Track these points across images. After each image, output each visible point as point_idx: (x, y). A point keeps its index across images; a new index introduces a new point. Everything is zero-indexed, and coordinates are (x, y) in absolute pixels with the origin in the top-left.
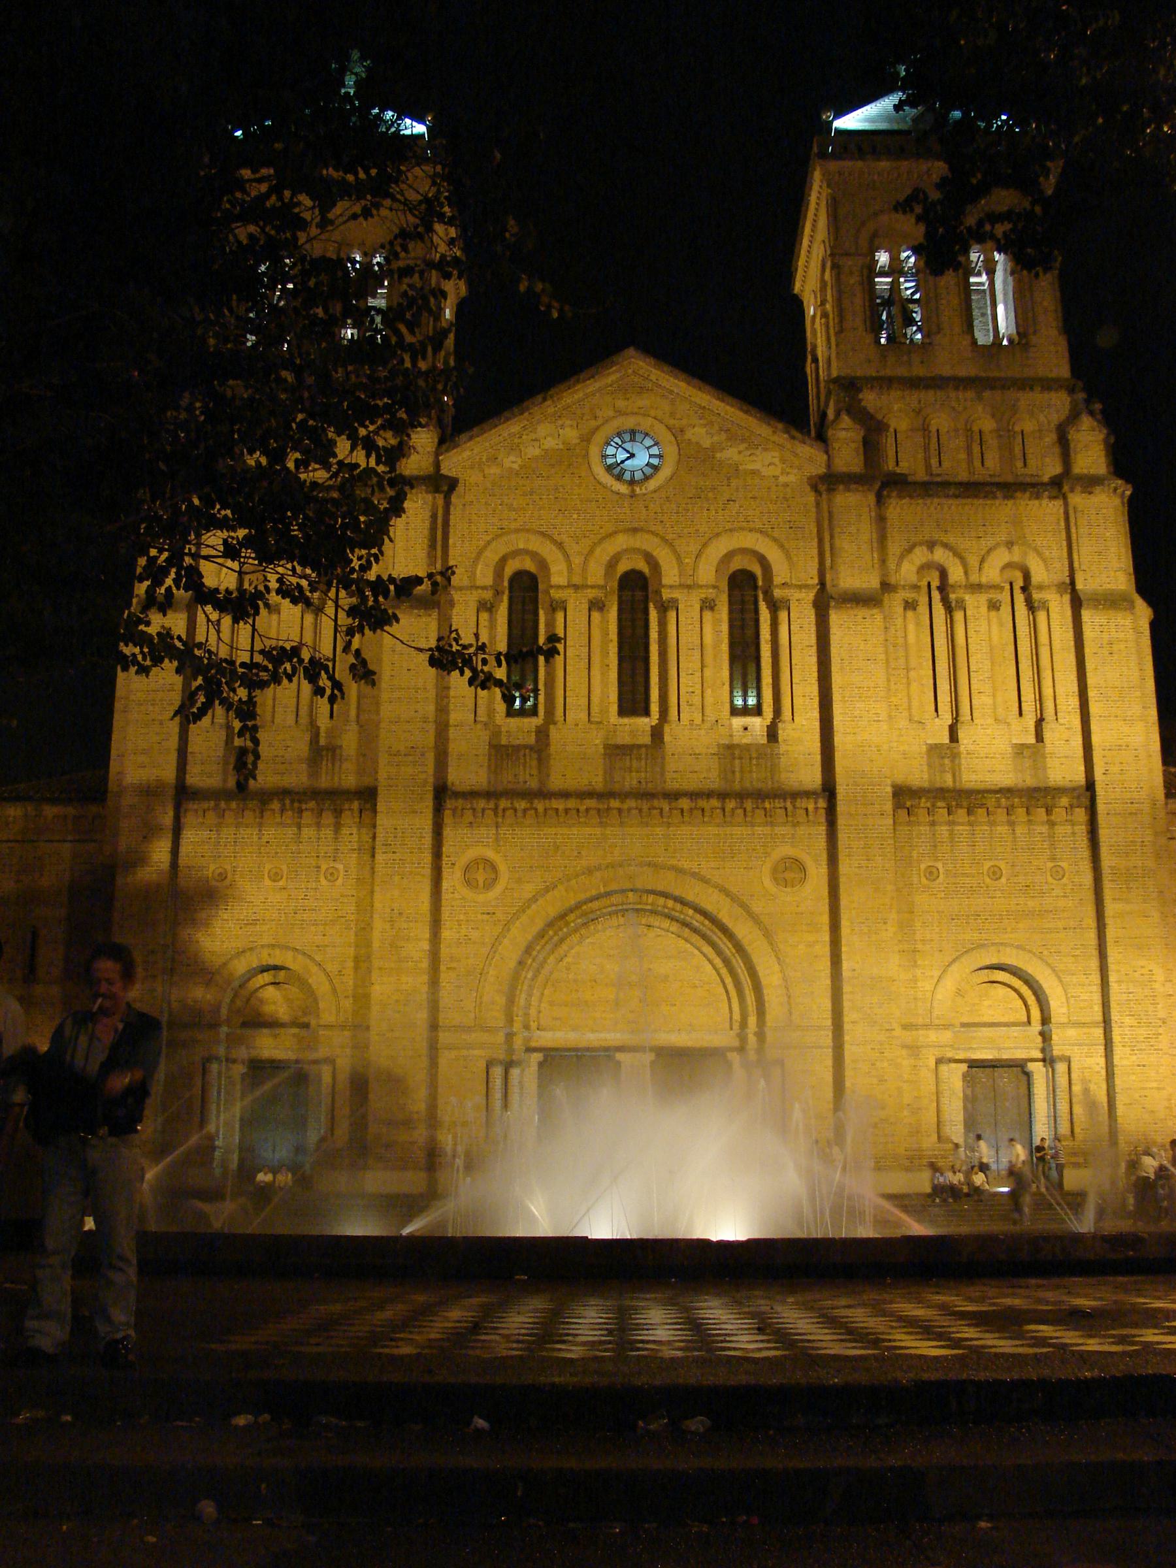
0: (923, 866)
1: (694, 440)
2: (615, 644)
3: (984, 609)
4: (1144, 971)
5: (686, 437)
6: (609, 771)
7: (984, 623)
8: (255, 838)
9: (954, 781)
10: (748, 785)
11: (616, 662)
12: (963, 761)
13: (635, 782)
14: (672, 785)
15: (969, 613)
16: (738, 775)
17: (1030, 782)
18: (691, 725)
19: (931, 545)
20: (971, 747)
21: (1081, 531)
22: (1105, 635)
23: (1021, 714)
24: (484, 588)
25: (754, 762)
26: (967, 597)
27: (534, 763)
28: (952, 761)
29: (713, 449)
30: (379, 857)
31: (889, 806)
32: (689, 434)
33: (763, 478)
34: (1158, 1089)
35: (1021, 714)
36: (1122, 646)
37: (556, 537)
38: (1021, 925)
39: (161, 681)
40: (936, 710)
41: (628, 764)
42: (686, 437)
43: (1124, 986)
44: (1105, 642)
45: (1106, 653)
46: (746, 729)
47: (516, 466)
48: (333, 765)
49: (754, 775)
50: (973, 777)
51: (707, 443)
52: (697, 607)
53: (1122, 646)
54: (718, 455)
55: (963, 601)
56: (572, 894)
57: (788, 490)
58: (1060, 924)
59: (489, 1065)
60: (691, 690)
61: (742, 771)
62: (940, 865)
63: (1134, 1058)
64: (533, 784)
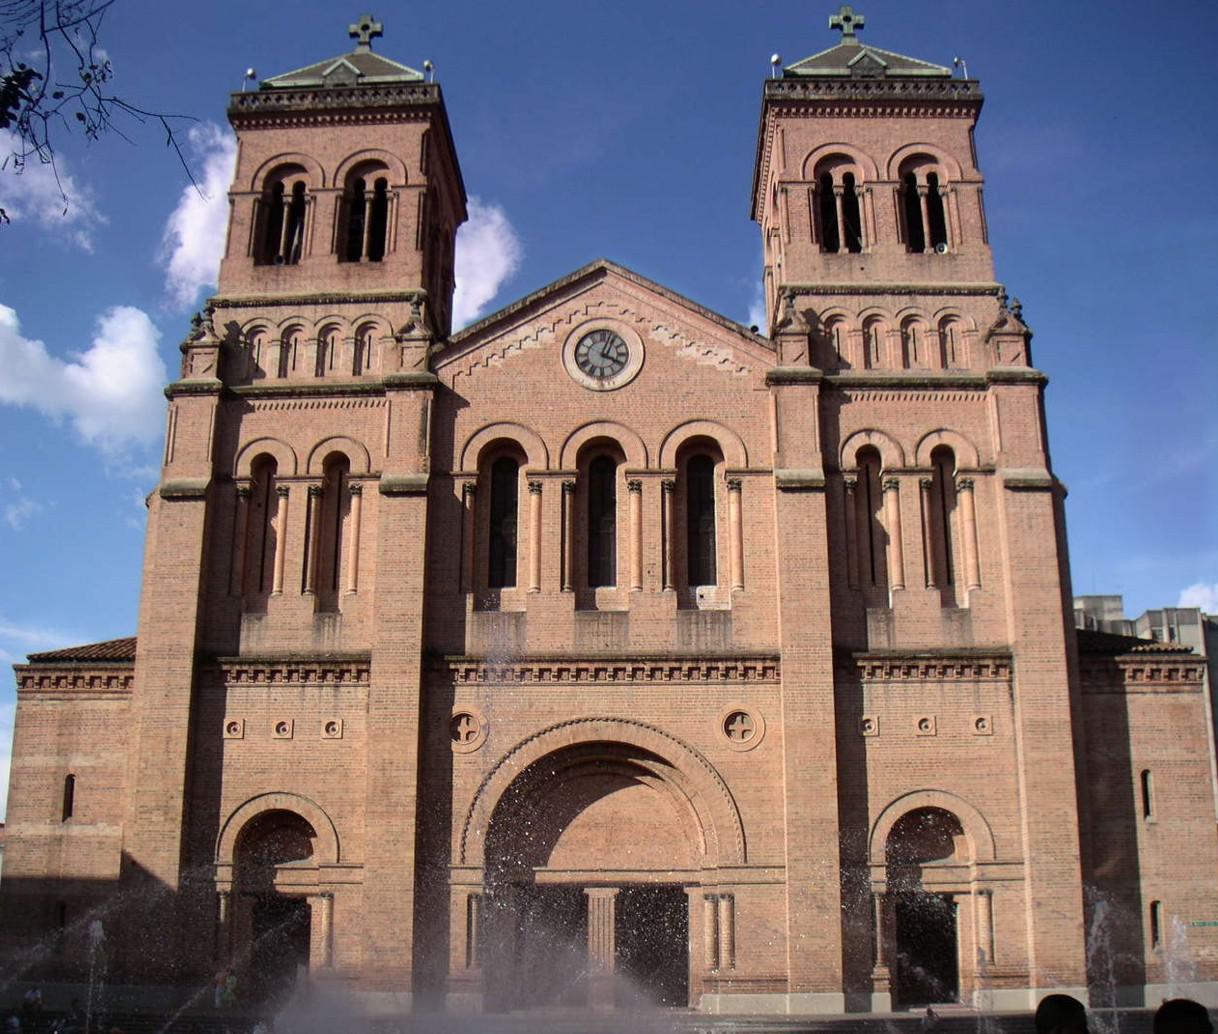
1: (657, 339)
2: (586, 522)
3: (916, 489)
4: (1061, 812)
5: (650, 337)
6: (581, 635)
8: (265, 696)
10: (703, 647)
11: (587, 538)
12: (897, 624)
13: (602, 646)
14: (633, 648)
15: (901, 492)
16: (694, 638)
19: (868, 431)
22: (1025, 509)
24: (470, 475)
25: (709, 626)
27: (513, 628)
28: (888, 625)
29: (674, 349)
30: (373, 712)
31: (829, 666)
32: (653, 335)
33: (718, 373)
34: (1071, 919)
36: (1040, 520)
37: (534, 427)
38: (948, 772)
39: (182, 557)
40: (873, 579)
42: (650, 337)
43: (1041, 826)
44: (1024, 516)
45: (1026, 527)
48: (334, 631)
49: (709, 638)
50: (906, 639)
51: (668, 343)
53: (1040, 520)
54: (678, 353)
55: (897, 483)
56: (545, 746)
57: (742, 383)
58: (984, 771)
59: (470, 898)
61: (698, 635)
63: (1049, 891)
64: (512, 645)
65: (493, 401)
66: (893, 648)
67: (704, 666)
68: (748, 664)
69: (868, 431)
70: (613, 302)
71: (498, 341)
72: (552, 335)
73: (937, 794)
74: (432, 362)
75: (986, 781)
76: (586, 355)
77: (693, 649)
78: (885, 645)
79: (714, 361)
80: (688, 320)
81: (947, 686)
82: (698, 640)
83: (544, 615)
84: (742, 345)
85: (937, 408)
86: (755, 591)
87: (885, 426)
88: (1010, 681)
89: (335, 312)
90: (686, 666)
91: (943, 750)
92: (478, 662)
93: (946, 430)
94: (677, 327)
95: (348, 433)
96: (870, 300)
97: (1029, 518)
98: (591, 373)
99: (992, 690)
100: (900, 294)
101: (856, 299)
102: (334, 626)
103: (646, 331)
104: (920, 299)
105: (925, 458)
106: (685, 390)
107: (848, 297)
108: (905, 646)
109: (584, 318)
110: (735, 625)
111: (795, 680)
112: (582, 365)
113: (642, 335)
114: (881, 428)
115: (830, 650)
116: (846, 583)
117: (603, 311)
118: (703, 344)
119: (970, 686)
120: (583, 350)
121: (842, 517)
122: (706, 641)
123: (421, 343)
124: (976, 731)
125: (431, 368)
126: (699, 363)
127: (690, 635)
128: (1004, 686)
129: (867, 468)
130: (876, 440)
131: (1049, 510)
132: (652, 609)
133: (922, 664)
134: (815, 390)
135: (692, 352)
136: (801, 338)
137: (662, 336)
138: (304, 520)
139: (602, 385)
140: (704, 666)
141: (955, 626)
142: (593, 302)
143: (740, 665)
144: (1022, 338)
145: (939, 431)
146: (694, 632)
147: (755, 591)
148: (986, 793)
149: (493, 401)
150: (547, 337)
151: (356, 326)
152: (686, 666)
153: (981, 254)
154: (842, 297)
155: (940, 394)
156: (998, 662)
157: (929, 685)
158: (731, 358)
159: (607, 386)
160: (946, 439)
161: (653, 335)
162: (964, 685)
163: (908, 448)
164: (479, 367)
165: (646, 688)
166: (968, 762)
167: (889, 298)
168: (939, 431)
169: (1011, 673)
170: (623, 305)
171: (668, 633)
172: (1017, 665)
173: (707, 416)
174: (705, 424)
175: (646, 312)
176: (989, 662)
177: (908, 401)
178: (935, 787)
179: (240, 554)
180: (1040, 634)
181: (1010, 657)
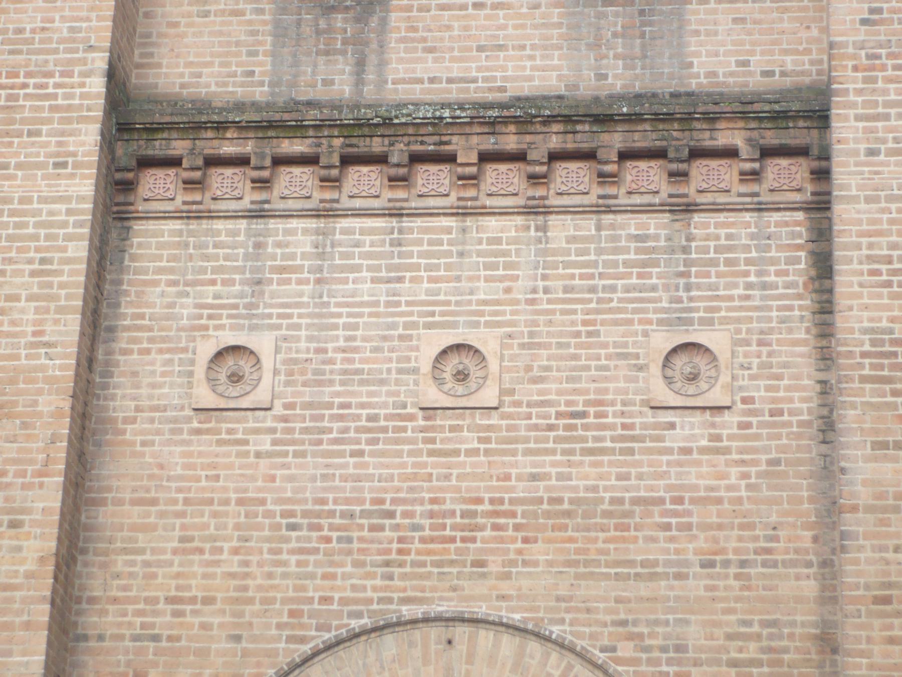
0: (206, 349)
9: (359, 82)
17: (615, 75)
38: (539, 552)
50: (426, 67)
58: (691, 549)
62: (263, 343)
66: (369, 93)
73: (485, 637)
75: (696, 587)
81: (561, 229)
88: (820, 206)
91: (524, 465)
99: (746, 246)
108: (417, 92)
115: (97, 85)
119: (656, 225)
128: (791, 227)
133: (466, 149)
148: (694, 635)
156: (771, 138)
157: (492, 222)
162: (631, 224)
166: (621, 516)
169: (822, 175)
172: (847, 131)
178: (482, 610)
181: (821, 118)
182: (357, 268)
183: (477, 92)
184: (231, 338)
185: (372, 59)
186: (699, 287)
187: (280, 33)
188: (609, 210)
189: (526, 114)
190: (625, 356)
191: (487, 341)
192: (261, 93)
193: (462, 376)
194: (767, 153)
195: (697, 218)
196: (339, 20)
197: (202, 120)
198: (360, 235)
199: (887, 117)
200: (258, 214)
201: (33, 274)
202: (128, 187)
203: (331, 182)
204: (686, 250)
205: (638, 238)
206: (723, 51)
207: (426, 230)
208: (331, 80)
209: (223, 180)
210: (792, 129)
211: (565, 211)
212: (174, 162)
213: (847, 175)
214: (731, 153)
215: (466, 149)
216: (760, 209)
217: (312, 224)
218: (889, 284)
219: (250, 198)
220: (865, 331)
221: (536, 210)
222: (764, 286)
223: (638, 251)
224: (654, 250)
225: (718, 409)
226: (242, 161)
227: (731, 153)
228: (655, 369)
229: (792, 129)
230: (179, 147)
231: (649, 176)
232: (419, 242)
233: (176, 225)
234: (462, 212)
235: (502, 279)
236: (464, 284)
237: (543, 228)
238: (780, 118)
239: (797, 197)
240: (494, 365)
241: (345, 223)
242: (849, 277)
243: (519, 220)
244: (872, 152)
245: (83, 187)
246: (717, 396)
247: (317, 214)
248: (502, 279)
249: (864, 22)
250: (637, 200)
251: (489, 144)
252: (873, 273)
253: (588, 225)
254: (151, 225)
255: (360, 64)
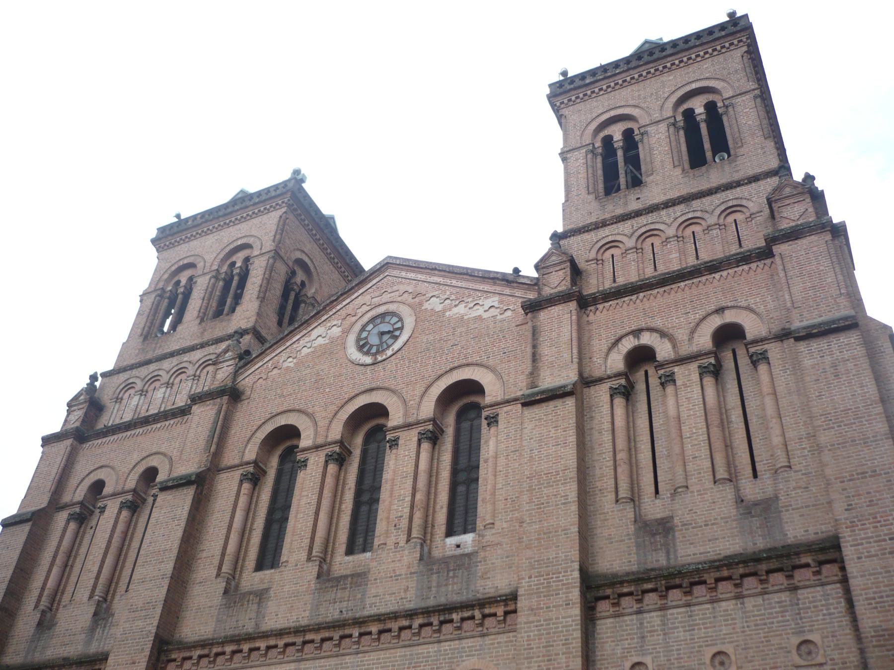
3: (695, 377)
7: (697, 389)
9: (668, 559)
17: (760, 543)
18: (396, 548)
20: (688, 517)
21: (790, 274)
22: (828, 359)
23: (755, 475)
25: (451, 574)
26: (676, 369)
27: (255, 606)
29: (444, 311)
32: (426, 306)
35: (755, 475)
41: (333, 596)
46: (458, 546)
47: (292, 365)
50: (691, 550)
51: (439, 308)
52: (416, 439)
53: (850, 365)
60: (400, 514)
64: (250, 627)
65: (282, 396)
66: (672, 562)
67: (435, 620)
68: (487, 611)
69: (636, 333)
70: (395, 288)
71: (295, 346)
72: (340, 329)
74: (236, 374)
76: (366, 338)
77: (431, 602)
78: (663, 562)
79: (479, 311)
80: (459, 284)
81: (750, 603)
82: (437, 592)
83: (286, 589)
84: (507, 291)
85: (711, 291)
86: (505, 525)
87: (658, 323)
88: (845, 581)
89: (185, 359)
90: (417, 622)
92: (212, 644)
93: (728, 308)
94: (448, 293)
95: (163, 450)
96: (642, 220)
97: (834, 366)
98: (367, 353)
99: (819, 601)
100: (674, 205)
101: (629, 223)
102: (105, 627)
103: (421, 304)
104: (696, 204)
105: (704, 340)
106: (450, 343)
107: (619, 225)
108: (689, 560)
109: (369, 308)
110: (481, 568)
111: (531, 619)
112: (360, 348)
113: (417, 309)
114: (653, 325)
115: (576, 574)
116: (612, 496)
117: (386, 298)
118: (470, 299)
119: (785, 596)
120: (364, 335)
121: (607, 426)
122: (452, 591)
123: (230, 363)
124: (798, 661)
125: (234, 380)
126: (466, 317)
127: (430, 588)
128: (835, 590)
129: (646, 372)
130: (646, 339)
131: (860, 351)
132: (392, 565)
133: (710, 578)
134: (573, 305)
135: (461, 309)
136: (563, 266)
137: (435, 304)
138: (109, 531)
139: (376, 359)
140: (435, 620)
141: (756, 522)
142: (377, 294)
143: (477, 614)
144: (808, 196)
145: (720, 310)
146: (434, 584)
147: (505, 525)
149: (282, 396)
150: (336, 331)
151: (197, 365)
152: (417, 622)
153: (762, 148)
154: (614, 226)
155: (717, 276)
156: (822, 557)
157: (724, 604)
158: (496, 305)
159: (380, 358)
160: (730, 317)
161: (426, 306)
162: (775, 598)
163: (681, 335)
164: (276, 371)
165: (373, 656)
167: (663, 213)
168: (720, 310)
169: (843, 569)
170: (402, 288)
171: (406, 590)
172: (848, 552)
173: (470, 360)
174: (467, 369)
175: (422, 288)
176: (806, 559)
177: (682, 292)
179: (55, 570)
180: (871, 503)
181: (837, 547)
182: (678, 627)
183: (711, 556)
184: (636, 659)
185: (672, 550)
186: (805, 618)
187: (638, 546)
188: (766, 593)
189: (729, 562)
190: (782, 648)
191: (729, 649)
192: (635, 568)
193: (722, 663)
194: (821, 563)
195: (799, 592)
196: (658, 538)
197: (615, 581)
198: (677, 615)
199: (862, 544)
200: (639, 612)
201: (563, 645)
202: (593, 608)
203: (664, 597)
204: (798, 604)
205: (778, 602)
206: (797, 528)
207: (700, 610)
208: (658, 560)
209: (626, 602)
210: (828, 552)
211: (749, 596)
212: (607, 597)
213: (852, 568)
214: (807, 565)
215: (710, 578)
216: (822, 585)
217: (659, 613)
218: (876, 608)
219: (636, 607)
220: (871, 627)
221: (739, 597)
222: (830, 614)
223: (780, 607)
224: (786, 606)
225: (821, 665)
226: (630, 594)
227: (807, 565)
228: (794, 652)
229: (828, 552)
230: (609, 592)
231: (778, 578)
232: (698, 615)
233: (611, 620)
234: (712, 602)
235: (730, 625)
236: (717, 629)
237: (743, 603)
238: (823, 550)
239: (836, 578)
240: (733, 658)
241: (670, 611)
242: (860, 607)
243: (734, 602)
244: (859, 558)
245: (576, 611)
246: (820, 659)
247: (660, 609)
248: (730, 625)
249: (846, 510)
250: (776, 588)
251: (718, 575)
252: (869, 604)
253: (759, 600)
254: (603, 621)
255: (668, 553)
